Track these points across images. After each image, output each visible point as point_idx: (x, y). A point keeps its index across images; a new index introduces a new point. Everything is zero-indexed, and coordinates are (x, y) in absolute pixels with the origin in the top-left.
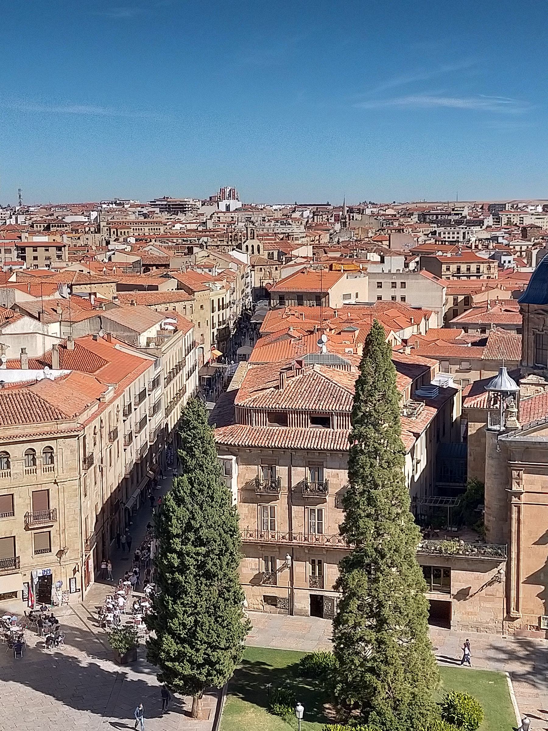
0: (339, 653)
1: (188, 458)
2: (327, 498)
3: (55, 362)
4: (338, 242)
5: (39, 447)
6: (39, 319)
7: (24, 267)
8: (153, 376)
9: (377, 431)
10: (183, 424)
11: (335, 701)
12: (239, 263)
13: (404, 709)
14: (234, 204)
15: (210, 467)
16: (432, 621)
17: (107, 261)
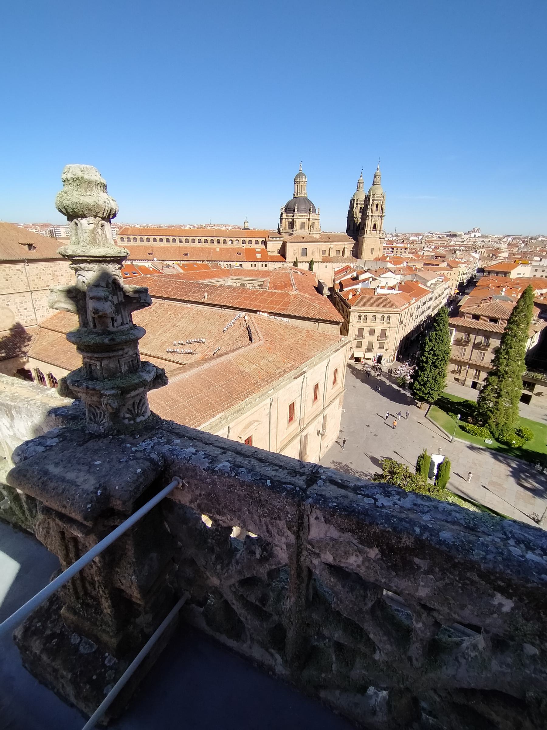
0: (479, 402)
1: (437, 326)
2: (489, 349)
3: (397, 288)
4: (521, 252)
5: (386, 315)
6: (394, 273)
7: (392, 255)
8: (430, 297)
9: (518, 328)
10: (438, 314)
11: (473, 417)
12: (474, 257)
13: (500, 427)
14: (478, 234)
15: (445, 331)
16: (521, 400)
17: (422, 254)
